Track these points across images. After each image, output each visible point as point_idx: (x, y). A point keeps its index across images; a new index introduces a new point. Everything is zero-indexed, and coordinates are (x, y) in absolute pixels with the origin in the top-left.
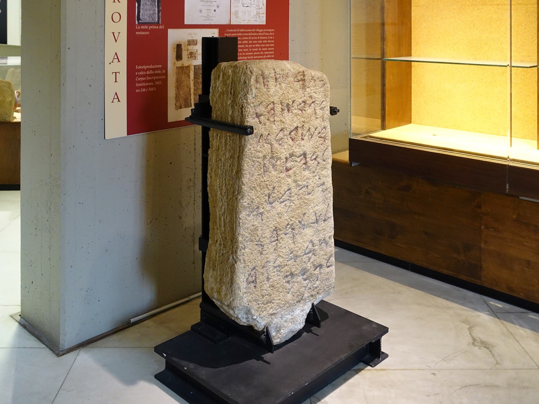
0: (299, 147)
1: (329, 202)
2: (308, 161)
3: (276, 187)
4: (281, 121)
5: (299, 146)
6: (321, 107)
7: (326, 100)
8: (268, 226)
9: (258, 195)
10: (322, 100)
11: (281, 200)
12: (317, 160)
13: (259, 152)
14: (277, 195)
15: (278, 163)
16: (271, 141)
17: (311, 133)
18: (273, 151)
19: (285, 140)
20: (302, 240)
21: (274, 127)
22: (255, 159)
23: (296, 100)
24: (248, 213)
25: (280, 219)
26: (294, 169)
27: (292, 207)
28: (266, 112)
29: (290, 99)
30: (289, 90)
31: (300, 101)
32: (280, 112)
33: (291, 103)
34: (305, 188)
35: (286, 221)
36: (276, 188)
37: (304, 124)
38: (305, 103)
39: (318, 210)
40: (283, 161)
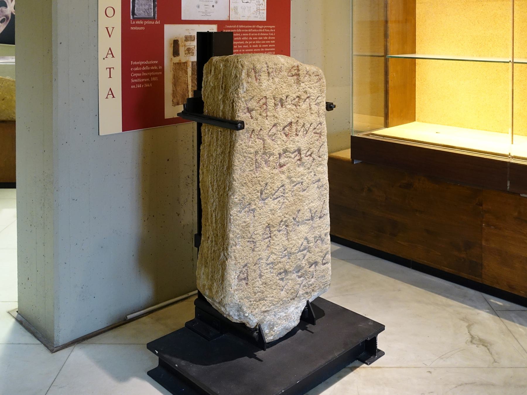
9: (249, 191)
11: (275, 196)
14: (270, 191)
36: (269, 184)
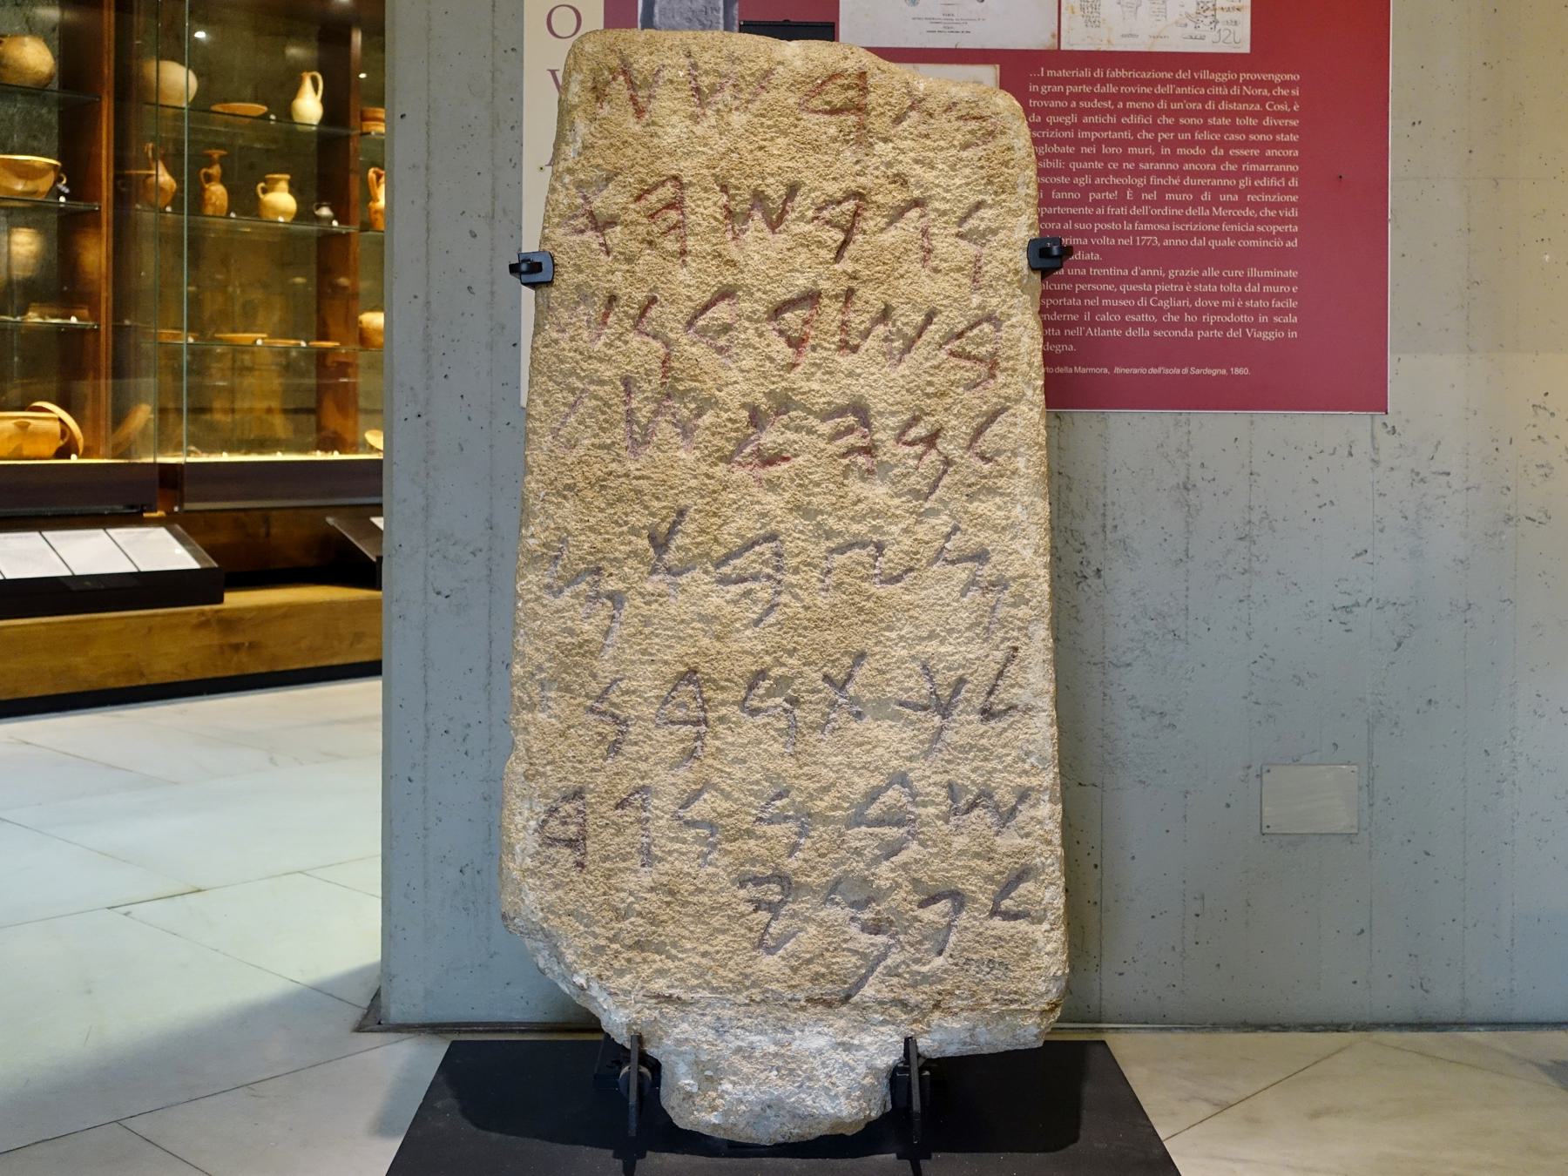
0: (824, 374)
2: (883, 442)
3: (692, 510)
4: (720, 255)
5: (827, 373)
6: (966, 227)
8: (644, 652)
10: (974, 199)
11: (726, 570)
12: (940, 448)
13: (601, 360)
15: (707, 419)
16: (662, 326)
17: (899, 330)
18: (672, 368)
19: (743, 336)
20: (840, 758)
21: (682, 275)
22: (579, 385)
23: (807, 182)
24: (547, 580)
25: (717, 644)
26: (800, 460)
27: (787, 610)
28: (638, 213)
29: (772, 175)
31: (833, 189)
32: (712, 221)
33: (775, 191)
34: (864, 552)
35: (749, 659)
37: (854, 284)
38: (867, 202)
40: (732, 416)
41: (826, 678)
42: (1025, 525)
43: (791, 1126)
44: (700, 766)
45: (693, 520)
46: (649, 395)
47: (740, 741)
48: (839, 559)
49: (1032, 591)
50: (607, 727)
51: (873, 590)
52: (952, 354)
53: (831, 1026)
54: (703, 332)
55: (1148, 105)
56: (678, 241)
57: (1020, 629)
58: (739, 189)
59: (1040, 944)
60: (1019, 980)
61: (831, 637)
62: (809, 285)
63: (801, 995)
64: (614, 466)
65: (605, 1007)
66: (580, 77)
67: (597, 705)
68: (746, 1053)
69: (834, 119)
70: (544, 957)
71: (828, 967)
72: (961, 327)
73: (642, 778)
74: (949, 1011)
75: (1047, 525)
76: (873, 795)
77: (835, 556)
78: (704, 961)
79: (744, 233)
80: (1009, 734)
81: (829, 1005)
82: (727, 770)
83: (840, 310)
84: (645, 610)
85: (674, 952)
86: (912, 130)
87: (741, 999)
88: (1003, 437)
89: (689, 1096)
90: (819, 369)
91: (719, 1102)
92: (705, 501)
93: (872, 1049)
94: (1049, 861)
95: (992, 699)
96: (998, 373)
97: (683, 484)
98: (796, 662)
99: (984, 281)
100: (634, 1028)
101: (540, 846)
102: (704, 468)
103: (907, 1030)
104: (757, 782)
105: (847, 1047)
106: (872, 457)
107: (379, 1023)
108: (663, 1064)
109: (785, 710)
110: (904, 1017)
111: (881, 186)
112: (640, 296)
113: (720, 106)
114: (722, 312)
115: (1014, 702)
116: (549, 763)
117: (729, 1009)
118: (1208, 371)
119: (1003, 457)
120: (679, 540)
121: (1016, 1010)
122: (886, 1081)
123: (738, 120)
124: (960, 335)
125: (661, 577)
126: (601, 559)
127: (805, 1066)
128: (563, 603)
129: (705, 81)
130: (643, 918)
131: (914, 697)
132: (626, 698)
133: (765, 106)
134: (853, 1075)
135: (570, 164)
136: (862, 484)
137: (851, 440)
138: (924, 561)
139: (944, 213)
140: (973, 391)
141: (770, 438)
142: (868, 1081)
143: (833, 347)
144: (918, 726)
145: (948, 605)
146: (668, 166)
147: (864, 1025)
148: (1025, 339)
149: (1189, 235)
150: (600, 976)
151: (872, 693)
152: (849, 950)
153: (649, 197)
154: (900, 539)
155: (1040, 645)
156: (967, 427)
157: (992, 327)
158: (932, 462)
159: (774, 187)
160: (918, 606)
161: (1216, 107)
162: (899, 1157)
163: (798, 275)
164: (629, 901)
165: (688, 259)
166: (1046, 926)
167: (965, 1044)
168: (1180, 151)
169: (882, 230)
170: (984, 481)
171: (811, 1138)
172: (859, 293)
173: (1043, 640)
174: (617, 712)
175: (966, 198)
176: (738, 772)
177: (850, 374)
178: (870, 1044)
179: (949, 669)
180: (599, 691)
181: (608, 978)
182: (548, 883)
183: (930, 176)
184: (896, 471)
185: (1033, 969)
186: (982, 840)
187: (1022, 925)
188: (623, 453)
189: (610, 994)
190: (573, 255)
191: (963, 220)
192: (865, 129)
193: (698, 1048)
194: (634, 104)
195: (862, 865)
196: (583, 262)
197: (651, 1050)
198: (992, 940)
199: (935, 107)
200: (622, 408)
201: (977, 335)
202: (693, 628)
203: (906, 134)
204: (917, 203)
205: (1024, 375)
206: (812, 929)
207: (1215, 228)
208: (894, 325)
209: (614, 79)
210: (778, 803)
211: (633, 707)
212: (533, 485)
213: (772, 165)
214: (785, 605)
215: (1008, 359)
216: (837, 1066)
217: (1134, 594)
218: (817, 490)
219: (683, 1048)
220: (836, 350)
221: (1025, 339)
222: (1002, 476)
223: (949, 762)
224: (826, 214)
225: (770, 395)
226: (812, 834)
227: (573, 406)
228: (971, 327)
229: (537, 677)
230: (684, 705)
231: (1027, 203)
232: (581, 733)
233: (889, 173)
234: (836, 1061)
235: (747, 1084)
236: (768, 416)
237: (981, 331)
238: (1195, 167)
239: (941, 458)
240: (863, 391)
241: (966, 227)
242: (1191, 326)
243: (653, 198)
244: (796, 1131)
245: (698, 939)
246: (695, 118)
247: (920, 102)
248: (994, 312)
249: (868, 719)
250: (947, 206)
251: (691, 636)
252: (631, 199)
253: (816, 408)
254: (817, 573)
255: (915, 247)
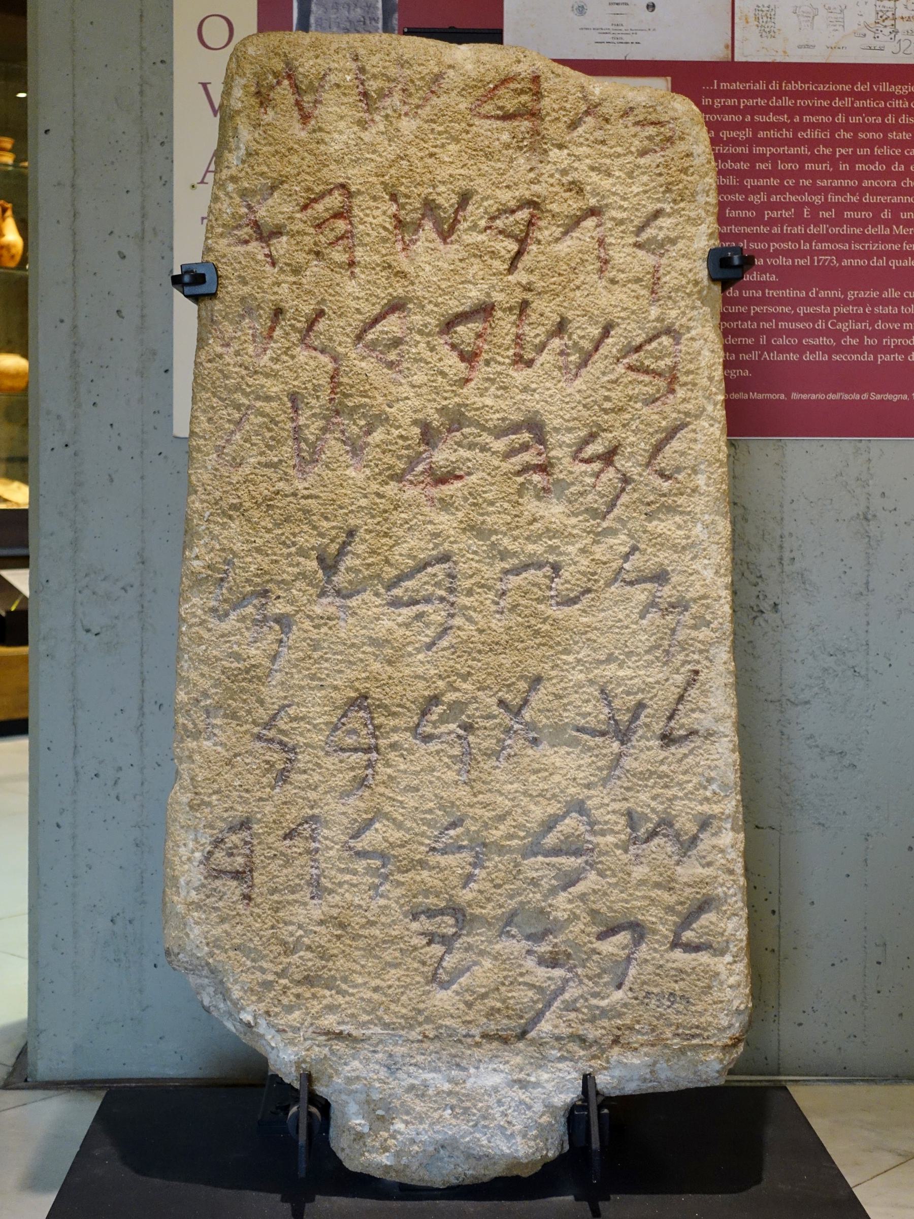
0: (497, 389)
1: (698, 662)
2: (559, 459)
4: (390, 266)
5: (501, 388)
7: (678, 212)
8: (313, 677)
9: (258, 540)
10: (652, 207)
12: (618, 465)
13: (267, 376)
14: (369, 565)
15: (378, 436)
16: (331, 339)
18: (341, 384)
20: (515, 785)
21: (351, 287)
23: (480, 190)
24: (213, 603)
25: (388, 668)
26: (473, 478)
27: (461, 633)
28: (305, 222)
29: (443, 183)
30: (443, 146)
31: (507, 197)
32: (381, 231)
33: (446, 200)
34: (540, 573)
35: (421, 684)
37: (528, 296)
39: (620, 681)
40: (404, 433)
41: (501, 703)
42: (706, 544)
43: (466, 1167)
44: (371, 795)
45: (364, 541)
46: (318, 411)
47: (413, 768)
48: (514, 581)
49: (713, 613)
50: (275, 755)
51: (550, 612)
52: (630, 368)
53: (507, 1062)
54: (372, 346)
55: (825, 119)
56: (346, 252)
57: (701, 652)
58: (408, 197)
59: (723, 977)
60: (701, 1014)
61: (506, 660)
62: (482, 297)
63: (476, 1031)
64: (281, 485)
65: (273, 1045)
66: (243, 81)
67: (264, 732)
68: (419, 1091)
69: (507, 124)
70: (209, 994)
71: (504, 1001)
72: (639, 340)
73: (312, 808)
74: (628, 1046)
75: (728, 545)
76: (550, 824)
77: (510, 577)
78: (376, 996)
79: (414, 243)
80: (690, 760)
81: (505, 1041)
82: (400, 798)
83: (514, 323)
84: (314, 634)
85: (344, 987)
86: (588, 136)
87: (414, 1035)
88: (683, 454)
89: (360, 1136)
90: (493, 384)
91: (391, 1142)
92: (376, 521)
93: (550, 1086)
94: (731, 891)
95: (672, 724)
96: (677, 387)
97: (353, 503)
98: (470, 687)
99: (663, 292)
100: (303, 1066)
101: (206, 878)
102: (374, 486)
103: (585, 1066)
104: (430, 811)
105: (523, 1084)
106: (548, 474)
107: (26, 1080)
108: (333, 1105)
109: (459, 737)
110: (582, 1053)
111: (556, 194)
112: (307, 309)
113: (389, 112)
114: (392, 325)
115: (696, 727)
116: (215, 793)
117: (402, 1046)
118: (888, 397)
119: (683, 474)
120: (349, 561)
121: (698, 1045)
122: (563, 1120)
123: (407, 126)
124: (638, 349)
125: (330, 599)
126: (268, 582)
127: (480, 1105)
128: (229, 627)
129: (373, 86)
130: (312, 952)
131: (591, 722)
132: (295, 725)
133: (436, 111)
134: (529, 1114)
135: (233, 171)
136: (537, 503)
137: (527, 457)
138: (602, 582)
139: (621, 222)
140: (652, 406)
141: (442, 456)
142: (545, 1119)
143: (507, 361)
144: (596, 752)
145: (627, 627)
146: (336, 174)
147: (541, 1062)
148: (706, 352)
149: (868, 255)
150: (268, 1013)
151: (548, 718)
152: (525, 984)
153: (316, 206)
154: (577, 559)
155: (722, 668)
156: (646, 444)
157: (671, 340)
158: (610, 480)
159: (445, 195)
160: (596, 628)
161: (897, 120)
162: (577, 1199)
163: (471, 286)
164: (298, 934)
165: (357, 270)
166: (728, 958)
167: (645, 1080)
168: (859, 167)
169: (557, 240)
170: (663, 499)
171: (486, 1180)
172: (534, 305)
173: (725, 663)
174: (285, 739)
175: (644, 206)
176: (411, 801)
177: (525, 389)
178: (547, 1081)
179: (628, 693)
180: (266, 718)
181: (277, 1014)
182: (214, 916)
183: (607, 184)
184: (573, 489)
185: (715, 1003)
186: (662, 869)
187: (704, 957)
188: (291, 472)
189: (278, 1031)
190: (237, 266)
191: (641, 229)
192: (539, 135)
193: (369, 1087)
194: (300, 110)
195: (538, 896)
196: (248, 274)
197: (321, 1090)
198: (673, 973)
199: (611, 112)
200: (289, 425)
201: (656, 349)
202: (364, 652)
203: (582, 140)
204: (593, 212)
205: (705, 389)
206: (487, 963)
207: (896, 247)
208: (570, 338)
209: (279, 83)
210: (452, 832)
211: (301, 734)
212: (197, 504)
213: (443, 173)
214: (459, 628)
215: (688, 373)
216: (513, 1104)
217: (813, 629)
218: (491, 509)
219: (353, 1087)
220: (510, 364)
221: (706, 352)
222: (682, 494)
223: (628, 789)
224: (499, 223)
225: (442, 411)
226: (487, 864)
227: (238, 423)
228: (650, 340)
229: (202, 704)
230: (354, 732)
231: (707, 212)
232: (247, 761)
233: (564, 181)
234: (513, 1099)
235: (421, 1123)
236: (440, 432)
237: (660, 344)
238: (875, 184)
239: (619, 476)
240: (538, 406)
241: (644, 236)
242: (871, 349)
243: (320, 207)
244: (471, 1172)
245: (369, 973)
246: (362, 124)
247: (596, 107)
248: (674, 324)
249: (544, 746)
250: (625, 215)
251: (362, 660)
252: (297, 208)
253: (490, 424)
254: (491, 595)
255: (591, 258)
